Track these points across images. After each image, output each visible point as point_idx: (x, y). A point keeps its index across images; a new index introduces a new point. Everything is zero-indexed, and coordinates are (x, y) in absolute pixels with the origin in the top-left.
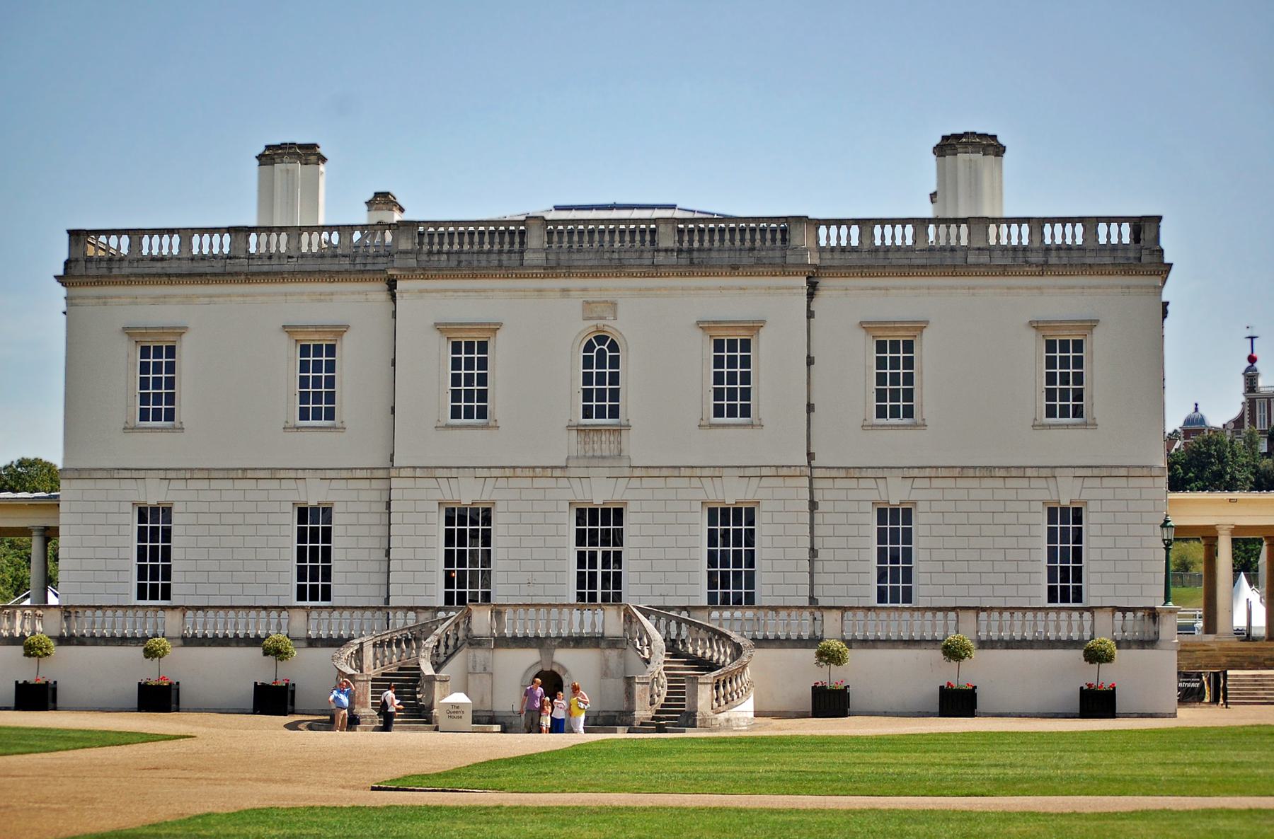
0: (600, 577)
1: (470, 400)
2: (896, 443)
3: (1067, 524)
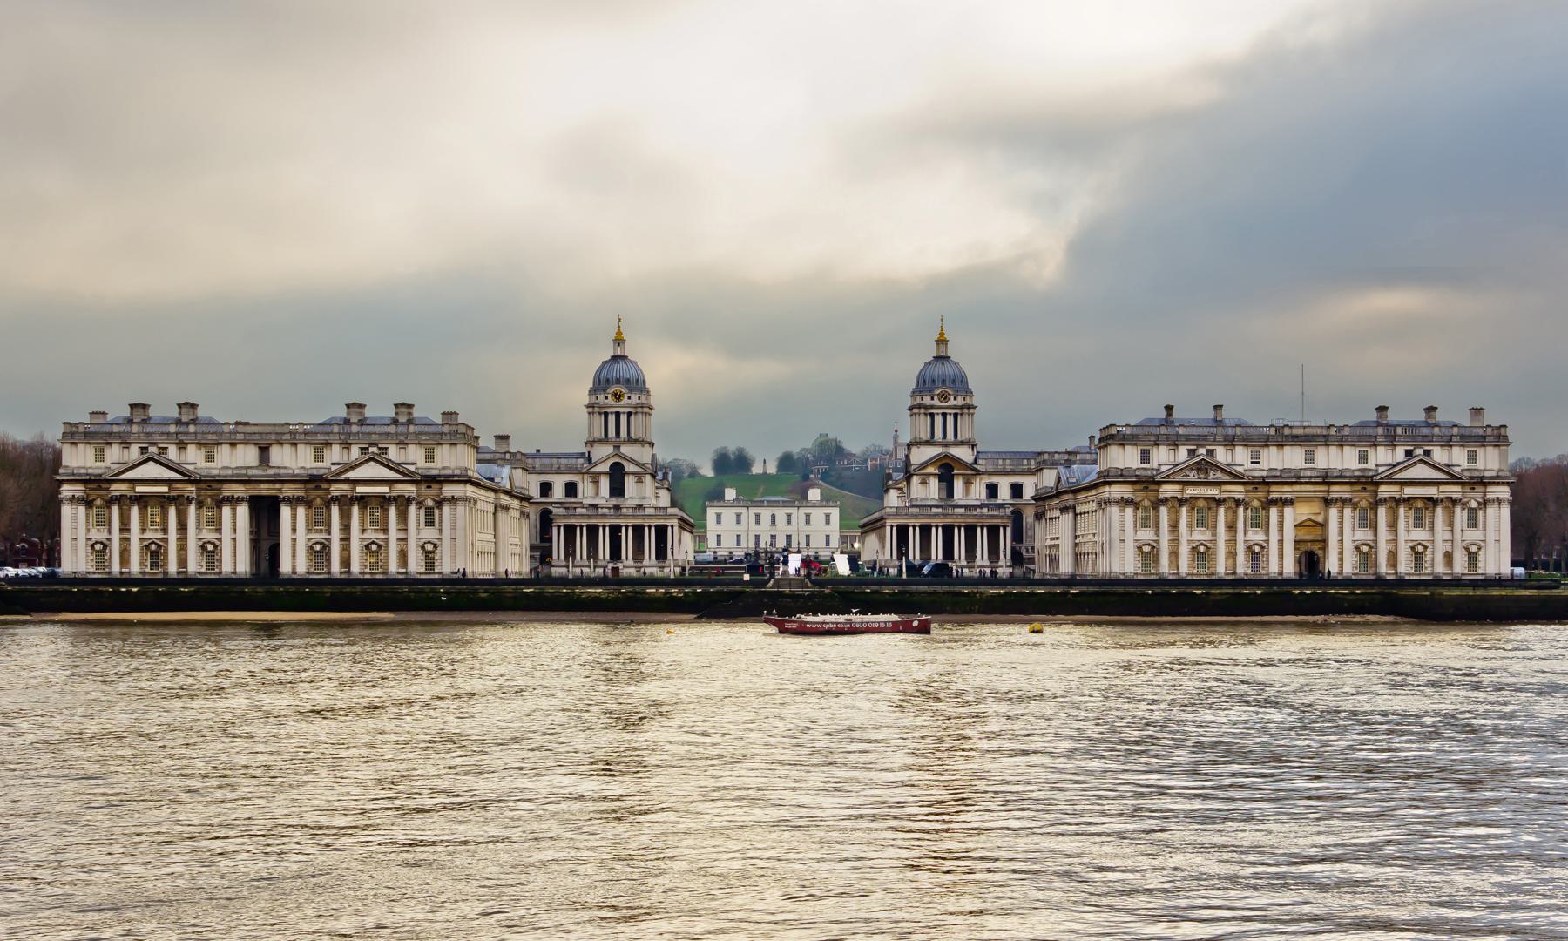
0: (773, 544)
1: (758, 522)
2: (808, 527)
3: (828, 537)
